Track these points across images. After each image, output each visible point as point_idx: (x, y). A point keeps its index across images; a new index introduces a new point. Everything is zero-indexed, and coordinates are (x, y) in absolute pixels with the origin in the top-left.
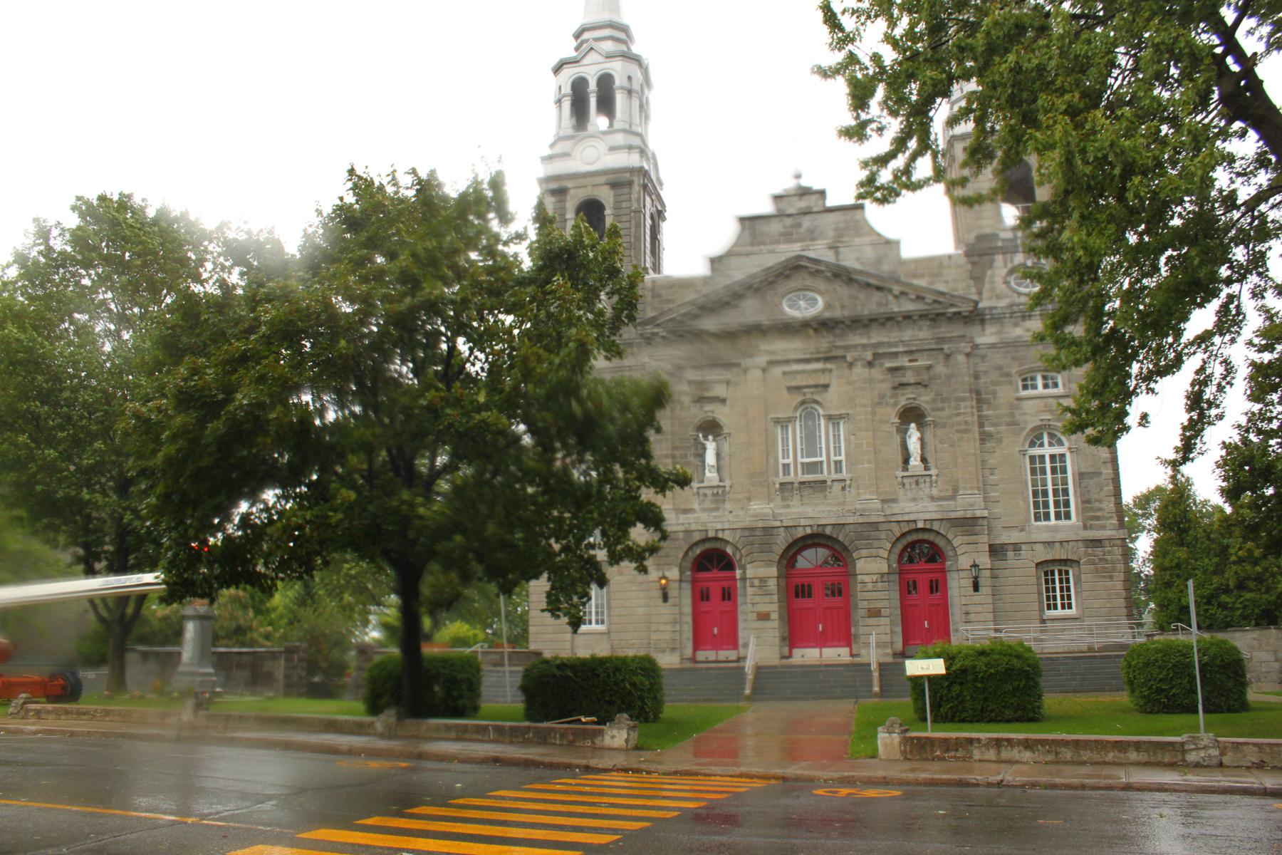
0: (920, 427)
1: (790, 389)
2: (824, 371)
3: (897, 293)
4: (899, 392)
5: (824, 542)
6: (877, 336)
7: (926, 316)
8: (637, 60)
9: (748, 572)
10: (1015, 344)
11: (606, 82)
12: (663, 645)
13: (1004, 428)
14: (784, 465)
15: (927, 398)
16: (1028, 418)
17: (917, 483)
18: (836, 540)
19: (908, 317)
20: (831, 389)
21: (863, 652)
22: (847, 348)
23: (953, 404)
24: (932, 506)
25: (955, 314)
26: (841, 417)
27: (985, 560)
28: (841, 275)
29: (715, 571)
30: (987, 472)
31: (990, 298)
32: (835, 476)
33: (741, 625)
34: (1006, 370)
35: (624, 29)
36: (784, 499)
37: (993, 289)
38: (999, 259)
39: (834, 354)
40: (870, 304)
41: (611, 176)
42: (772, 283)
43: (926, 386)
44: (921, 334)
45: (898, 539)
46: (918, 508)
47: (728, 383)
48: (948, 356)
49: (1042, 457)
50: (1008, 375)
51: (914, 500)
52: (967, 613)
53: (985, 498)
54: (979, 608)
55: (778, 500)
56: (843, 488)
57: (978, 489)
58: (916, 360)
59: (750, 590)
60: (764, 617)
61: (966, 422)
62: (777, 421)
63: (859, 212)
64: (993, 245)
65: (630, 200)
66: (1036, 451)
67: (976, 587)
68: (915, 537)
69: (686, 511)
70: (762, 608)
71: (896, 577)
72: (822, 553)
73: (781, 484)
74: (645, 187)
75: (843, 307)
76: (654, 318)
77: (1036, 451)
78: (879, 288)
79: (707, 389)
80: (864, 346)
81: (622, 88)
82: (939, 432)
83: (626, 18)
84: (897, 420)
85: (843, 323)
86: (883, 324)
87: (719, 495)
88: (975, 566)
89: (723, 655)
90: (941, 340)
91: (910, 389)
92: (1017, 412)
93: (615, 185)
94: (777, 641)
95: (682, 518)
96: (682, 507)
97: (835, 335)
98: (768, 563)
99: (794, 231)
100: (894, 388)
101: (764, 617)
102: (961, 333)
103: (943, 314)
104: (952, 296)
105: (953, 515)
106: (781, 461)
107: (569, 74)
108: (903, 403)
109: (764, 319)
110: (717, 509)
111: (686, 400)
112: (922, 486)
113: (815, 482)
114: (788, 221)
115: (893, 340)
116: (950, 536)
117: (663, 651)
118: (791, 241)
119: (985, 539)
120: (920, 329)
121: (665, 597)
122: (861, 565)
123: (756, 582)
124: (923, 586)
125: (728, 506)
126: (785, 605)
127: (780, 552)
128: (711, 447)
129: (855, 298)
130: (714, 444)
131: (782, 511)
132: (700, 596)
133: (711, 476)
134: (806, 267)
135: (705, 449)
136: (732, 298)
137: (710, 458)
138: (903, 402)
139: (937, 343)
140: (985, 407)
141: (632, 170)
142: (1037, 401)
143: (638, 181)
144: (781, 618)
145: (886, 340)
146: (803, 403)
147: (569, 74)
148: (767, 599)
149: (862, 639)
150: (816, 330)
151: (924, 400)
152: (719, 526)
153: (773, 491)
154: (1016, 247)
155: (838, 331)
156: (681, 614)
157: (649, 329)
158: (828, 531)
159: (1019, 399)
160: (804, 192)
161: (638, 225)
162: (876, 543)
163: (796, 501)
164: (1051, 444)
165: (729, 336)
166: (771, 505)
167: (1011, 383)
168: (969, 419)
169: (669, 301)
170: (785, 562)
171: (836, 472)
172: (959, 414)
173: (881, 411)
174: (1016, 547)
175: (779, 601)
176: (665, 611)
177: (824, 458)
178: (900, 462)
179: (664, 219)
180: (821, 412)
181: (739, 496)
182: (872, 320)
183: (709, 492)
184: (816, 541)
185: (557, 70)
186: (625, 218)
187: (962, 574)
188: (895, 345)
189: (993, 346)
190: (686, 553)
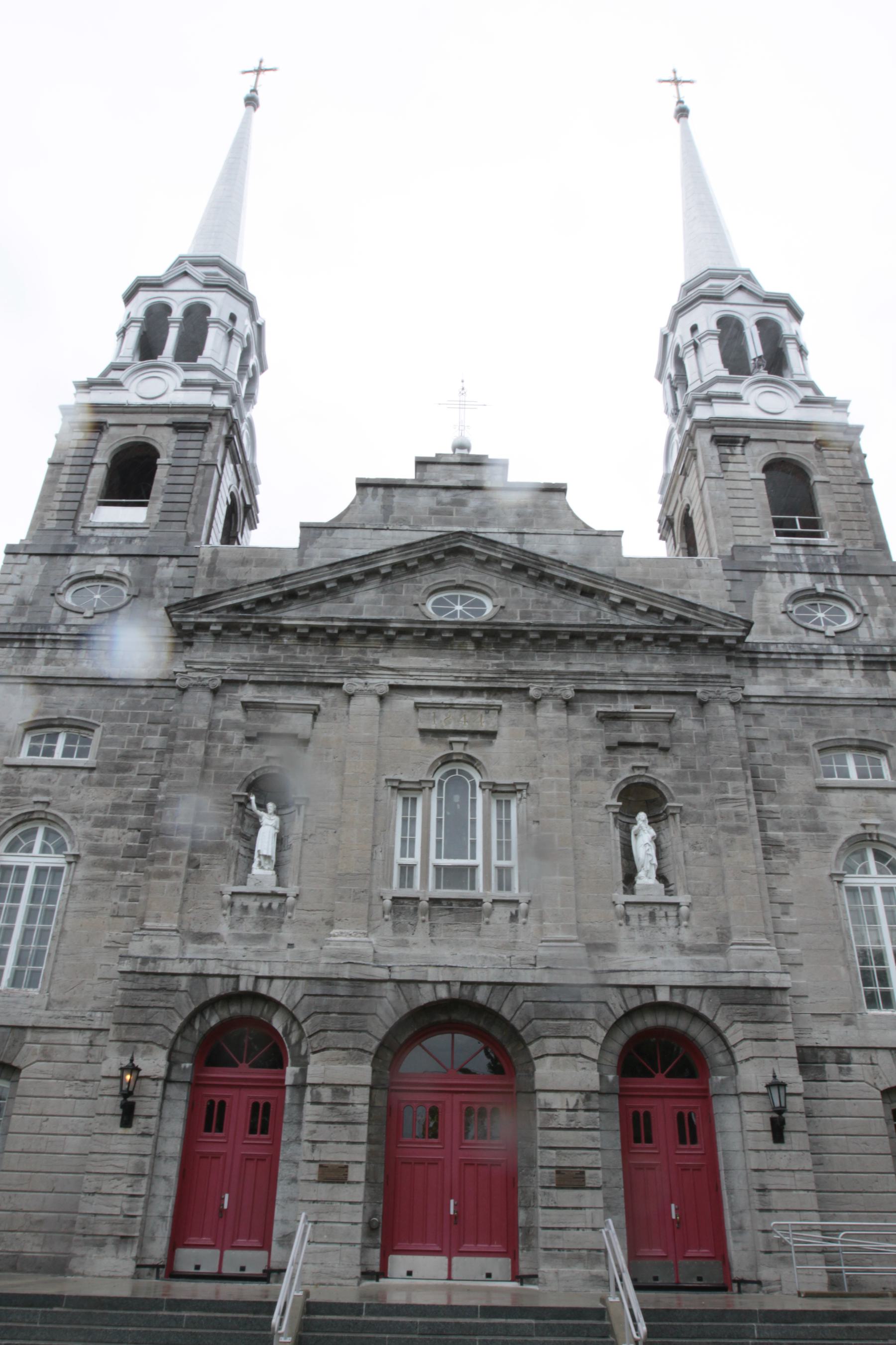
0: (653, 821)
1: (423, 732)
2: (488, 708)
3: (618, 600)
4: (618, 755)
5: (472, 1020)
6: (581, 662)
7: (664, 638)
8: (249, 302)
9: (310, 1069)
10: (809, 702)
11: (197, 318)
12: (104, 1229)
13: (799, 834)
14: (403, 867)
15: (668, 770)
16: (840, 821)
17: (652, 917)
18: (495, 1016)
19: (634, 638)
20: (497, 741)
21: (546, 1269)
22: (530, 675)
23: (715, 783)
24: (682, 962)
25: (712, 639)
26: (514, 790)
27: (791, 1075)
28: (529, 569)
29: (244, 1067)
30: (778, 909)
31: (764, 632)
32: (495, 893)
33: (283, 1190)
34: (796, 740)
35: (239, 276)
36: (396, 928)
37: (766, 620)
38: (773, 580)
39: (507, 685)
40: (574, 613)
41: (180, 418)
42: (413, 570)
43: (665, 750)
44: (658, 666)
45: (619, 1023)
46: (659, 963)
47: (316, 713)
48: (702, 704)
49: (868, 891)
50: (800, 748)
51: (647, 948)
52: (763, 1190)
53: (779, 954)
54: (787, 1181)
55: (387, 929)
56: (514, 917)
57: (766, 934)
58: (650, 708)
59: (310, 1112)
60: (333, 1174)
61: (738, 815)
62: (398, 787)
63: (556, 496)
64: (764, 558)
65: (201, 449)
66: (855, 880)
67: (778, 1130)
68: (649, 1021)
69: (201, 938)
70: (331, 1154)
71: (613, 1103)
72: (466, 1044)
73: (395, 899)
74: (228, 441)
75: (524, 615)
76: (204, 599)
77: (855, 880)
78: (588, 593)
79: (273, 721)
80: (560, 675)
81: (217, 322)
82: (694, 831)
83: (244, 262)
84: (614, 802)
85: (523, 634)
86: (592, 645)
87: (273, 908)
88: (777, 1085)
89: (235, 1260)
90: (689, 678)
91: (638, 753)
92: (820, 810)
93: (178, 427)
94: (357, 1234)
95: (192, 950)
96: (196, 928)
97: (508, 655)
98: (356, 1054)
99: (454, 509)
100: (610, 749)
101: (333, 1174)
102: (724, 672)
103: (693, 638)
104: (709, 610)
105: (725, 980)
106: (398, 859)
107: (144, 298)
108: (628, 775)
109: (397, 615)
110: (265, 938)
111: (236, 737)
112: (662, 923)
113: (460, 901)
114: (446, 496)
115: (606, 670)
116: (720, 1022)
117: (100, 1244)
118: (450, 523)
119: (788, 1032)
120: (655, 659)
121: (128, 1115)
122: (546, 1072)
123: (326, 1094)
124: (664, 1126)
125: (287, 934)
126: (381, 1149)
127: (382, 1033)
128: (269, 825)
129: (548, 604)
130: (276, 819)
131: (394, 951)
132: (206, 1117)
133: (262, 875)
134: (471, 552)
135: (257, 826)
136: (345, 579)
137: (265, 842)
138: (625, 772)
139: (683, 683)
140: (765, 796)
141: (211, 411)
142: (854, 794)
143: (219, 429)
144: (369, 1180)
145: (596, 669)
146: (446, 760)
147: (144, 298)
148: (344, 1133)
149: (543, 1239)
150: (478, 643)
151: (663, 771)
152: (264, 970)
153: (380, 912)
154: (799, 564)
155: (517, 650)
156: (156, 1156)
157: (194, 617)
158: (481, 996)
159: (822, 788)
160: (477, 462)
161: (207, 483)
162: (576, 1028)
163: (421, 934)
164: (880, 871)
165: (329, 637)
166: (373, 939)
167: (806, 761)
168: (743, 809)
169: (236, 582)
170: (389, 1056)
171: (500, 888)
172: (725, 800)
173: (586, 785)
174: (842, 1055)
175: (370, 1141)
176: (124, 1144)
177: (479, 861)
178: (620, 878)
179: (253, 526)
180: (477, 779)
181: (311, 917)
182: (574, 636)
183: (253, 904)
184: (456, 1016)
185: (128, 298)
186: (186, 471)
187: (748, 1103)
188: (613, 678)
189: (773, 701)
190: (189, 1022)
